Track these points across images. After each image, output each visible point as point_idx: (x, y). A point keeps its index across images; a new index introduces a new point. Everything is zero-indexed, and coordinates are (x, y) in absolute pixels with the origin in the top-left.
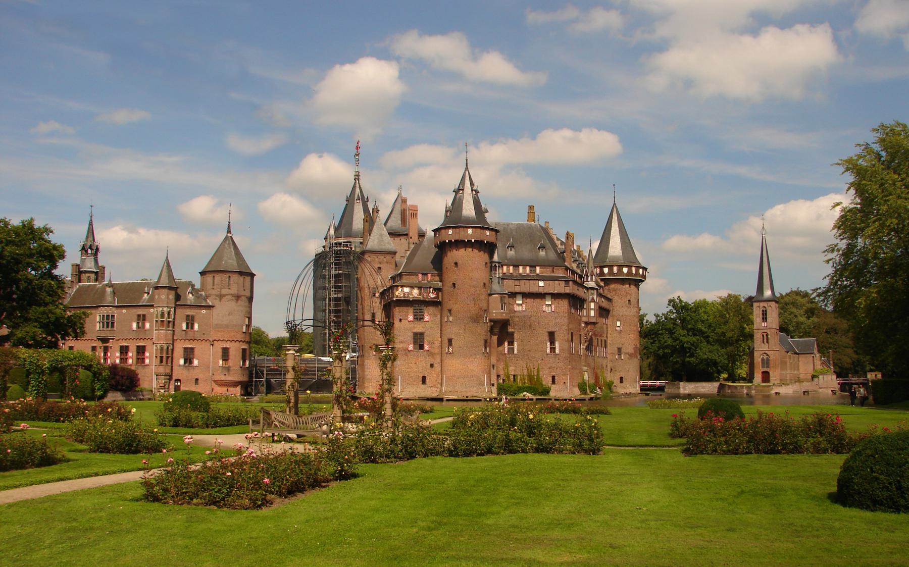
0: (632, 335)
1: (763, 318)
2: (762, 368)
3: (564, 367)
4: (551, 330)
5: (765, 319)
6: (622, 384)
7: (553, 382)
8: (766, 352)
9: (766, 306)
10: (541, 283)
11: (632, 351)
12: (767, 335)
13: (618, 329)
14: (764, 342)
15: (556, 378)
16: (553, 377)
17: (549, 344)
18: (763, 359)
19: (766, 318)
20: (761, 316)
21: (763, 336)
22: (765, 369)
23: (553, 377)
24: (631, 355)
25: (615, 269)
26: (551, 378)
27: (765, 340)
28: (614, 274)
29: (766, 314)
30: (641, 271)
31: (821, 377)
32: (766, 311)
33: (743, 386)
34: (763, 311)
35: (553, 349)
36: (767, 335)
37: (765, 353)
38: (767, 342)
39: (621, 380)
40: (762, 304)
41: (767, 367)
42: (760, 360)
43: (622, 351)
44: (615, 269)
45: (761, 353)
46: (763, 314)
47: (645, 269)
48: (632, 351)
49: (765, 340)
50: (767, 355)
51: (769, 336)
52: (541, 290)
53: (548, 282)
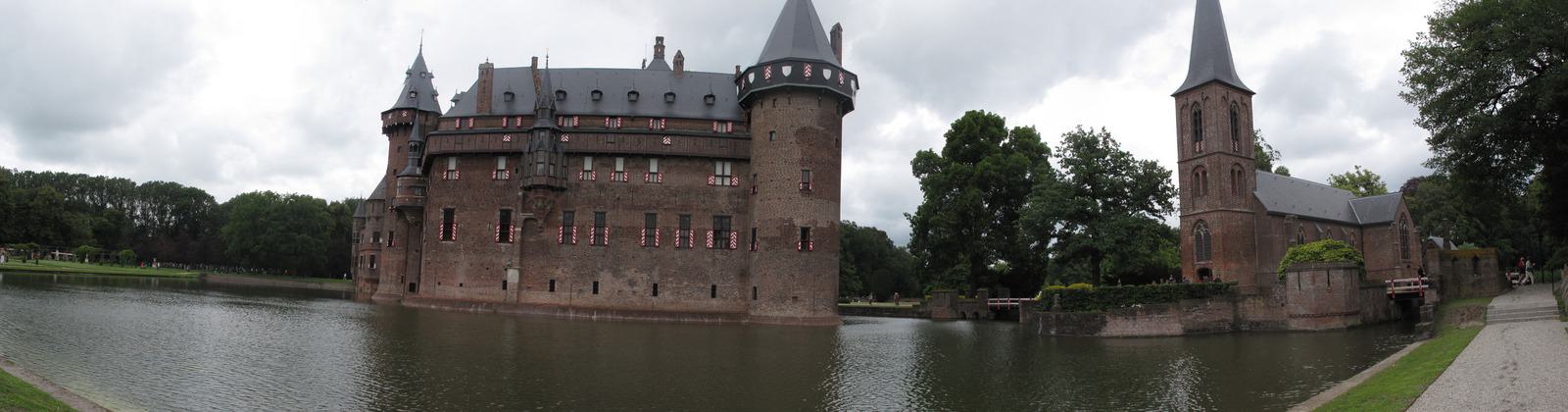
8: (1202, 217)
9: (1199, 100)
18: (1198, 236)
21: (1197, 175)
24: (772, 242)
27: (1201, 187)
32: (1200, 112)
34: (1195, 114)
36: (1204, 173)
49: (1201, 187)
51: (1208, 175)
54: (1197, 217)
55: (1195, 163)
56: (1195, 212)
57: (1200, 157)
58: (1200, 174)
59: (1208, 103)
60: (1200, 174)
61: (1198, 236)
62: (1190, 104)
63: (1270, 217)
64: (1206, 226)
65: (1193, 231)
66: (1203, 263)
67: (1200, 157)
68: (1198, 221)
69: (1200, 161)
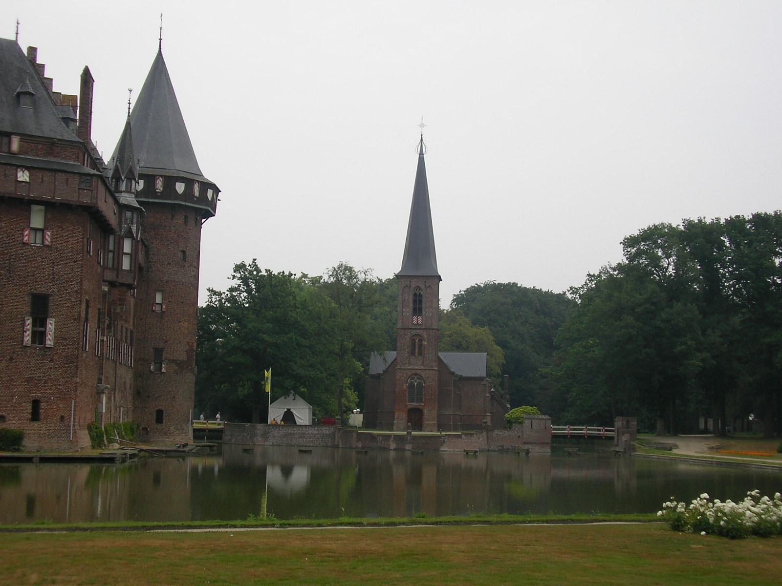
0: (186, 324)
1: (415, 309)
2: (409, 402)
3: (62, 381)
4: (42, 289)
6: (159, 426)
7: (35, 416)
8: (418, 372)
9: (423, 286)
10: (23, 176)
11: (183, 357)
12: (420, 340)
13: (157, 308)
15: (43, 405)
16: (36, 403)
17: (29, 322)
18: (411, 386)
19: (420, 310)
20: (411, 305)
22: (415, 404)
23: (36, 403)
24: (181, 366)
25: (159, 185)
26: (29, 406)
27: (417, 350)
28: (155, 194)
29: (421, 301)
30: (210, 193)
32: (420, 295)
33: (389, 436)
34: (415, 295)
35: (39, 336)
36: (420, 340)
37: (416, 374)
38: (420, 354)
39: (160, 417)
40: (414, 283)
41: (420, 400)
42: (405, 386)
43: (165, 355)
44: (159, 185)
45: (409, 374)
46: (415, 301)
48: (183, 357)
49: (417, 350)
50: (420, 377)
51: (425, 343)
52: (22, 193)
53: (40, 174)
54: (413, 372)
55: (414, 332)
58: (417, 341)
60: (417, 341)
61: (411, 386)
62: (413, 286)
64: (419, 379)
66: (414, 404)
68: (412, 375)
69: (418, 331)
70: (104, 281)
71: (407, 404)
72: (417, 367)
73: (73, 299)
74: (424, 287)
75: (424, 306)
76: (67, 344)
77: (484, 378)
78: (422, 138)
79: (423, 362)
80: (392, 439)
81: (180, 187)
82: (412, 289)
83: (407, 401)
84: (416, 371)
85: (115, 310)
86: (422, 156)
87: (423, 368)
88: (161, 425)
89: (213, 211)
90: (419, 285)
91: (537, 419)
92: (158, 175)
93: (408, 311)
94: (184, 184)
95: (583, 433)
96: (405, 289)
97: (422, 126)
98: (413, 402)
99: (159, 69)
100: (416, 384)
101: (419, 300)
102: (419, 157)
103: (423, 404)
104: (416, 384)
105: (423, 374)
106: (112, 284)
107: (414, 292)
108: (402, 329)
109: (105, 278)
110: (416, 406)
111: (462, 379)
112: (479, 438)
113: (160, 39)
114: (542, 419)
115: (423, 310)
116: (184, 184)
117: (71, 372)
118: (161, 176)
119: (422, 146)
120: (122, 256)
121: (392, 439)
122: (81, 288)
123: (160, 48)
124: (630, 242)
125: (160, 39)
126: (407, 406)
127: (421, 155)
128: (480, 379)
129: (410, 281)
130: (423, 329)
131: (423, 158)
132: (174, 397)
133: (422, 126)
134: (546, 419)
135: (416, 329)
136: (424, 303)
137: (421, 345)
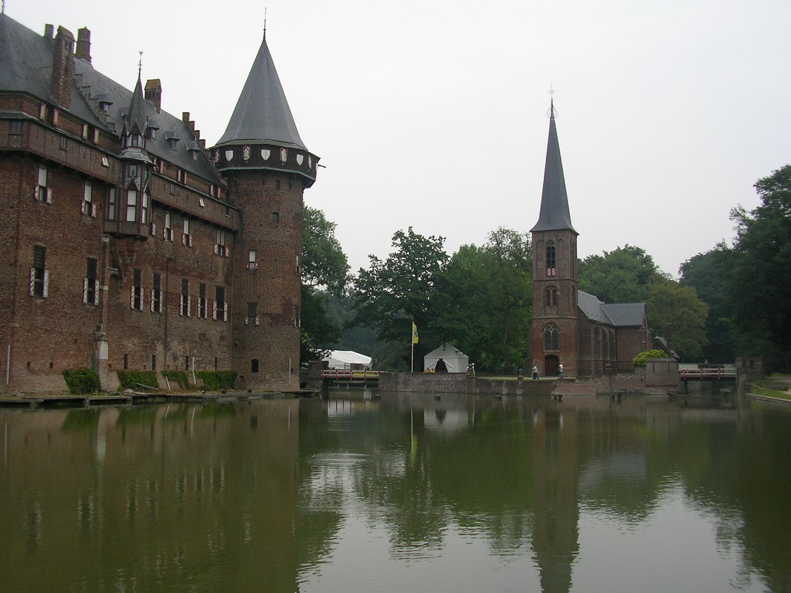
0: (280, 281)
1: (548, 262)
5: (551, 263)
6: (255, 375)
8: (553, 321)
9: (554, 240)
12: (554, 291)
13: (252, 266)
14: (549, 304)
18: (548, 334)
19: (554, 261)
20: (545, 258)
25: (247, 154)
28: (243, 163)
29: (554, 254)
31: (649, 366)
33: (502, 382)
34: (548, 248)
36: (554, 291)
37: (551, 323)
38: (555, 303)
39: (255, 366)
42: (541, 335)
43: (258, 309)
44: (247, 154)
45: (545, 323)
46: (548, 255)
47: (316, 159)
50: (555, 326)
51: (558, 293)
54: (549, 321)
56: (546, 317)
57: (552, 280)
58: (551, 291)
59: (561, 243)
61: (548, 334)
62: (546, 240)
63: (589, 323)
64: (554, 327)
65: (543, 329)
67: (552, 280)
70: (105, 233)
71: (545, 351)
72: (552, 317)
73: (9, 244)
74: (556, 240)
75: (556, 258)
76: (3, 289)
77: (641, 326)
78: (552, 104)
79: (557, 311)
80: (504, 384)
81: (266, 154)
82: (545, 243)
83: (544, 348)
84: (551, 320)
85: (125, 261)
86: (552, 119)
87: (557, 317)
88: (256, 373)
89: (313, 177)
90: (551, 239)
91: (659, 362)
92: (245, 145)
93: (542, 264)
94: (270, 151)
95: (717, 375)
96: (539, 244)
97: (552, 92)
98: (550, 349)
99: (264, 53)
100: (551, 332)
101: (552, 253)
102: (551, 121)
103: (558, 351)
104: (551, 332)
105: (557, 322)
106: (113, 235)
107: (547, 246)
108: (536, 281)
109: (106, 230)
110: (552, 353)
111: (617, 328)
112: (597, 382)
113: (265, 30)
114: (664, 362)
115: (556, 261)
116: (270, 151)
117: (7, 317)
118: (248, 145)
119: (552, 110)
120: (127, 208)
121: (504, 384)
122: (18, 233)
123: (264, 37)
124: (764, 185)
125: (265, 30)
126: (544, 353)
127: (552, 117)
128: (637, 327)
129: (543, 236)
130: (556, 280)
131: (554, 121)
132: (269, 348)
133: (552, 92)
134: (669, 362)
135: (550, 280)
136: (556, 254)
137: (555, 296)
